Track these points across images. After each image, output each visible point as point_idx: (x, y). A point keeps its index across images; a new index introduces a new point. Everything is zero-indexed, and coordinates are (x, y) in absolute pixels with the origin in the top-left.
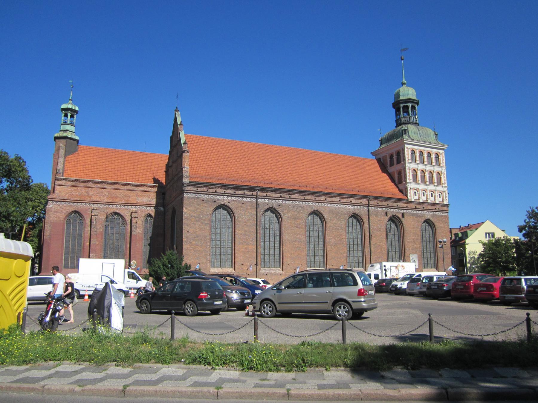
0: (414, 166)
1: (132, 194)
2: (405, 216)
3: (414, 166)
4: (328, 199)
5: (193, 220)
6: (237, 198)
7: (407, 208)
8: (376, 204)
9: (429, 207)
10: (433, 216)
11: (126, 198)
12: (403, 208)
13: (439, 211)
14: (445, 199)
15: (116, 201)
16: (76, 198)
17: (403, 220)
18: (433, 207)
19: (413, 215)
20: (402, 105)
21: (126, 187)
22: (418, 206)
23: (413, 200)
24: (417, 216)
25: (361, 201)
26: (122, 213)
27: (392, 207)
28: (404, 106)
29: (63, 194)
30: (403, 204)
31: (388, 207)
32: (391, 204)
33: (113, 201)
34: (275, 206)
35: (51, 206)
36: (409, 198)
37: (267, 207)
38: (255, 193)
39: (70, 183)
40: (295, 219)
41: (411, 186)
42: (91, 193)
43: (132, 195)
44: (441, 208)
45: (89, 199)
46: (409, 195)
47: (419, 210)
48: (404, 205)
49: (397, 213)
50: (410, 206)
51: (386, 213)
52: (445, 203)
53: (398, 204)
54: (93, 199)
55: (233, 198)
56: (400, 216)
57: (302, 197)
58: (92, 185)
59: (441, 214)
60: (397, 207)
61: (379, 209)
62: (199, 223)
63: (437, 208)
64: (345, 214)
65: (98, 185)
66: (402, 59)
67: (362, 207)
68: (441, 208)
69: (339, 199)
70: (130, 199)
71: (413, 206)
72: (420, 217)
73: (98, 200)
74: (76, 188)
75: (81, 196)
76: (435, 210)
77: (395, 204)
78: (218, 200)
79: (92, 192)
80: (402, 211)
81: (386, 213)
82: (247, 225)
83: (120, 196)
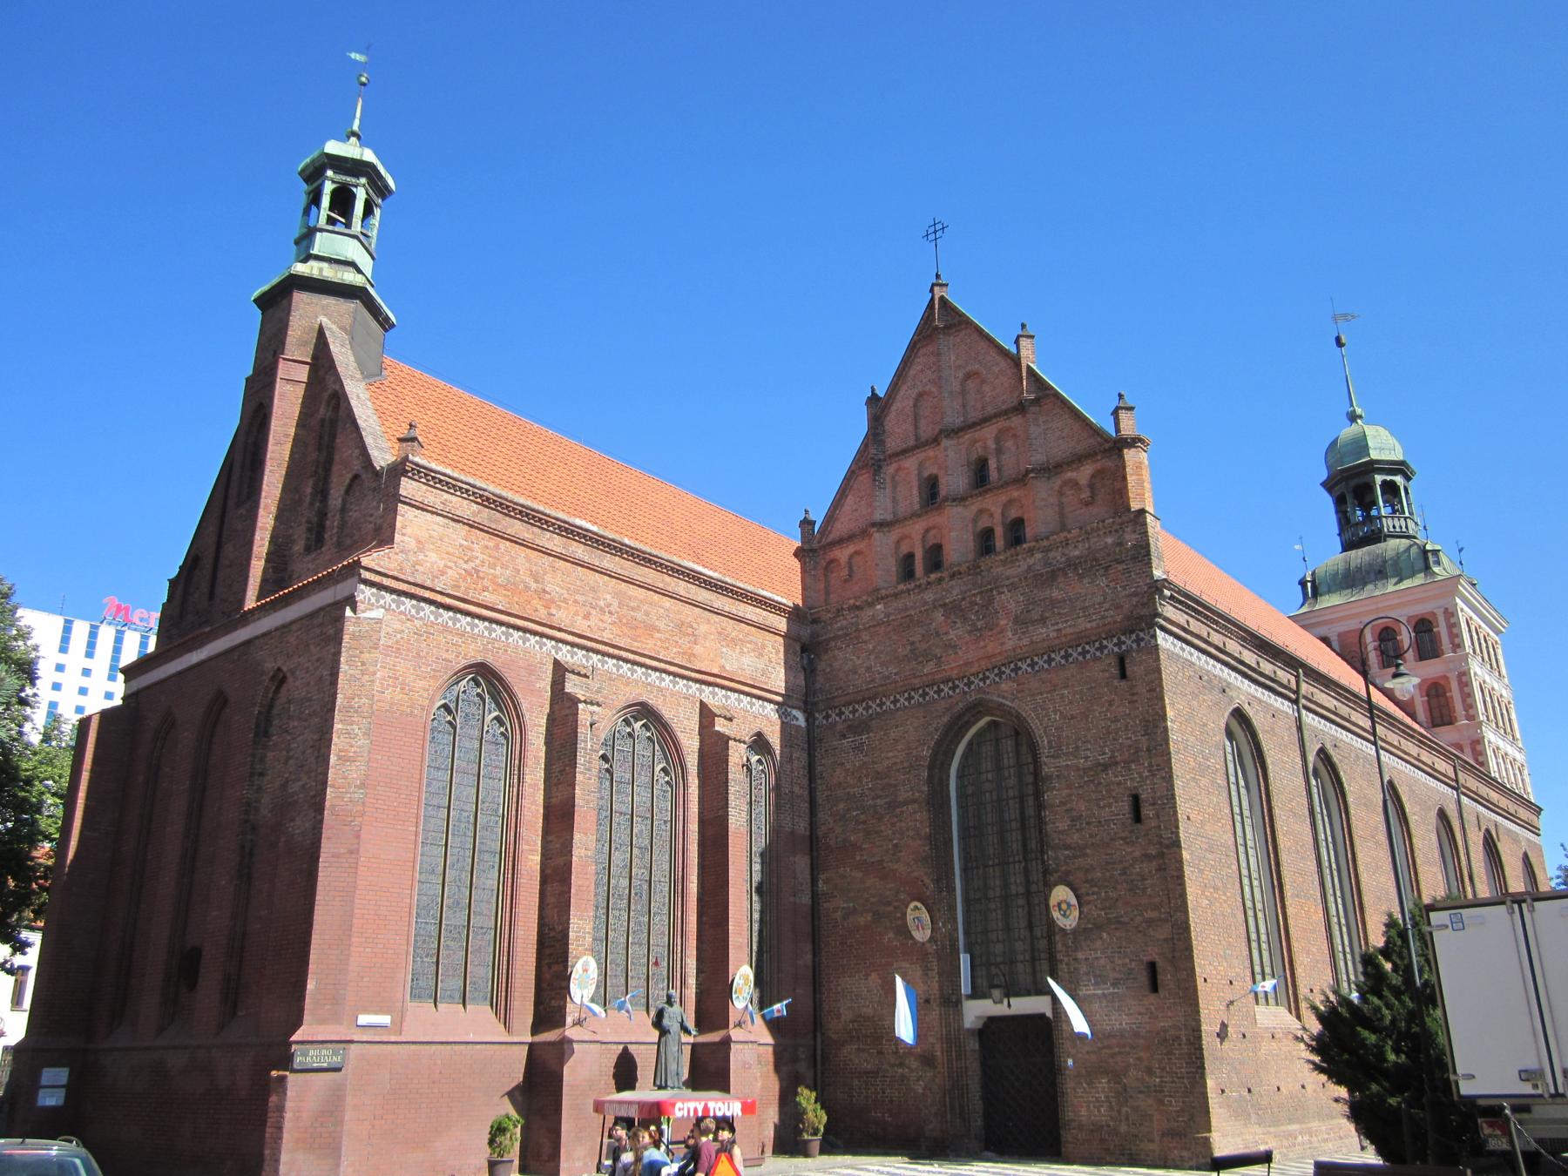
1: (707, 626)
11: (684, 642)
15: (648, 646)
16: (487, 597)
20: (1379, 479)
21: (681, 587)
26: (667, 713)
28: (1384, 483)
29: (433, 558)
33: (635, 646)
35: (377, 613)
39: (468, 509)
42: (554, 586)
43: (703, 628)
45: (542, 615)
54: (562, 617)
58: (555, 542)
65: (579, 551)
66: (1339, 343)
70: (698, 649)
73: (581, 626)
74: (491, 542)
75: (510, 587)
79: (558, 579)
83: (661, 625)
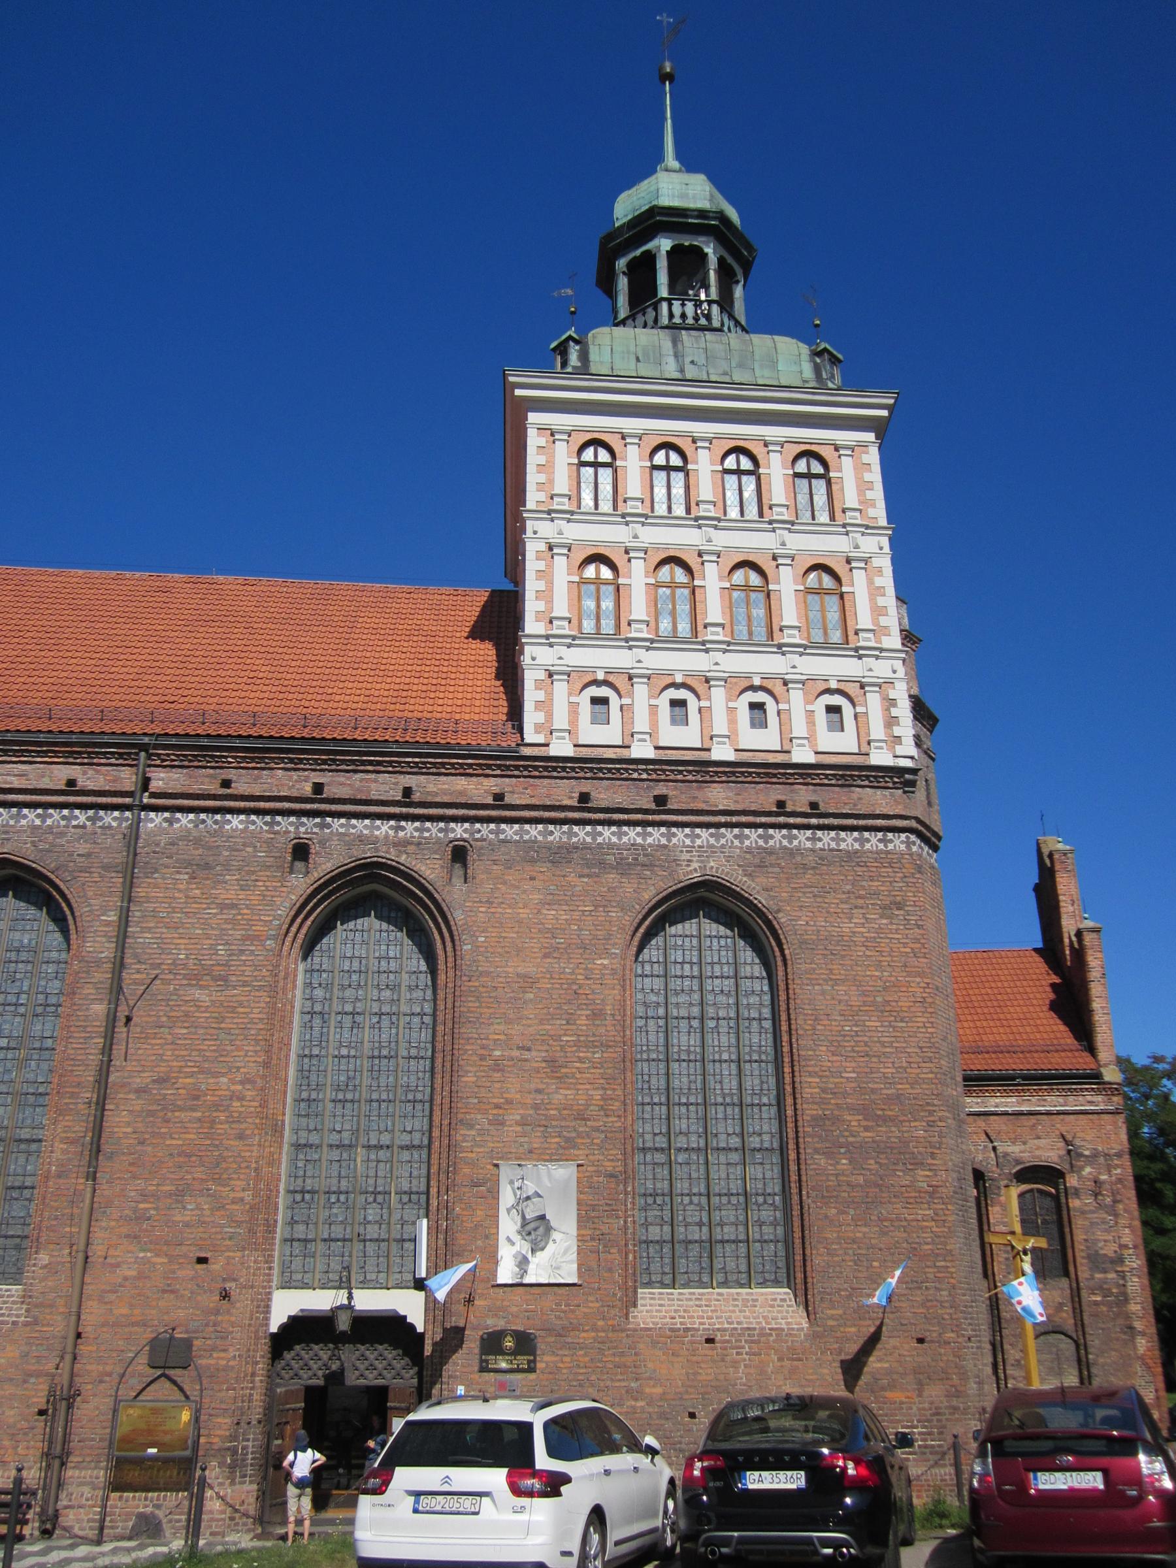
2: (476, 864)
7: (499, 810)
8: (214, 788)
9: (719, 796)
10: (761, 860)
12: (470, 812)
13: (816, 817)
14: (877, 731)
17: (455, 895)
18: (764, 797)
19: (560, 855)
22: (604, 794)
23: (561, 748)
24: (597, 861)
30: (461, 783)
31: (318, 805)
32: (340, 784)
44: (834, 799)
47: (615, 817)
48: (478, 789)
49: (406, 843)
50: (519, 791)
51: (301, 852)
52: (880, 757)
56: (430, 869)
59: (849, 841)
60: (408, 807)
63: (800, 797)
67: (81, 817)
68: (834, 799)
71: (564, 792)
76: (780, 816)
77: (385, 786)
80: (459, 831)
81: (301, 852)
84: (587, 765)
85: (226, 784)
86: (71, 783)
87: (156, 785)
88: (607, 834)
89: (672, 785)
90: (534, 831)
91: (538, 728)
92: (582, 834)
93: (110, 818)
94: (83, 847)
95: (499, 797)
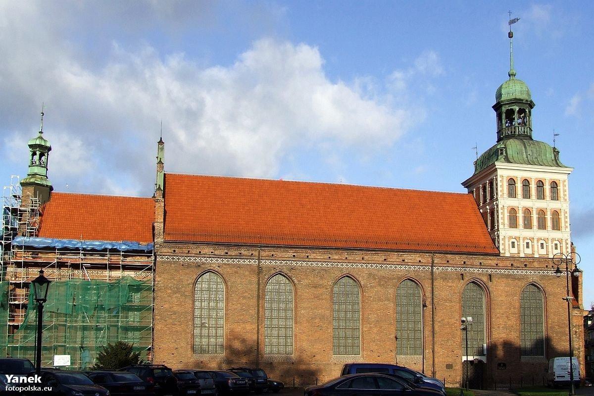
0: (513, 202)
3: (513, 202)
4: (366, 257)
5: (170, 291)
6: (231, 261)
10: (543, 277)
12: (491, 267)
19: (508, 276)
23: (507, 255)
25: (420, 259)
27: (472, 266)
30: (490, 262)
34: (285, 270)
36: (501, 251)
37: (273, 272)
38: (256, 253)
40: (315, 287)
41: (505, 232)
46: (501, 247)
53: (481, 261)
55: (225, 261)
56: (485, 279)
57: (326, 256)
61: (449, 269)
62: (177, 295)
64: (394, 279)
66: (510, 35)
69: (384, 258)
72: (519, 279)
78: (203, 264)
80: (489, 271)
82: (244, 298)
84: (512, 258)
85: (448, 261)
86: (420, 261)
87: (435, 262)
88: (515, 271)
89: (527, 262)
90: (503, 271)
91: (503, 249)
92: (511, 272)
93: (427, 268)
94: (423, 275)
95: (497, 265)
